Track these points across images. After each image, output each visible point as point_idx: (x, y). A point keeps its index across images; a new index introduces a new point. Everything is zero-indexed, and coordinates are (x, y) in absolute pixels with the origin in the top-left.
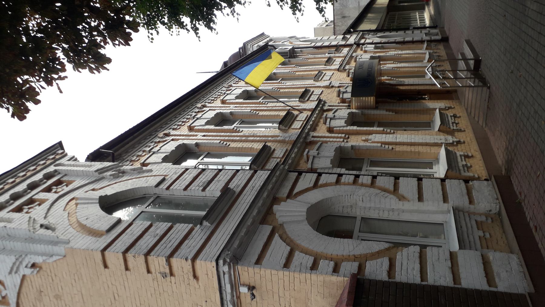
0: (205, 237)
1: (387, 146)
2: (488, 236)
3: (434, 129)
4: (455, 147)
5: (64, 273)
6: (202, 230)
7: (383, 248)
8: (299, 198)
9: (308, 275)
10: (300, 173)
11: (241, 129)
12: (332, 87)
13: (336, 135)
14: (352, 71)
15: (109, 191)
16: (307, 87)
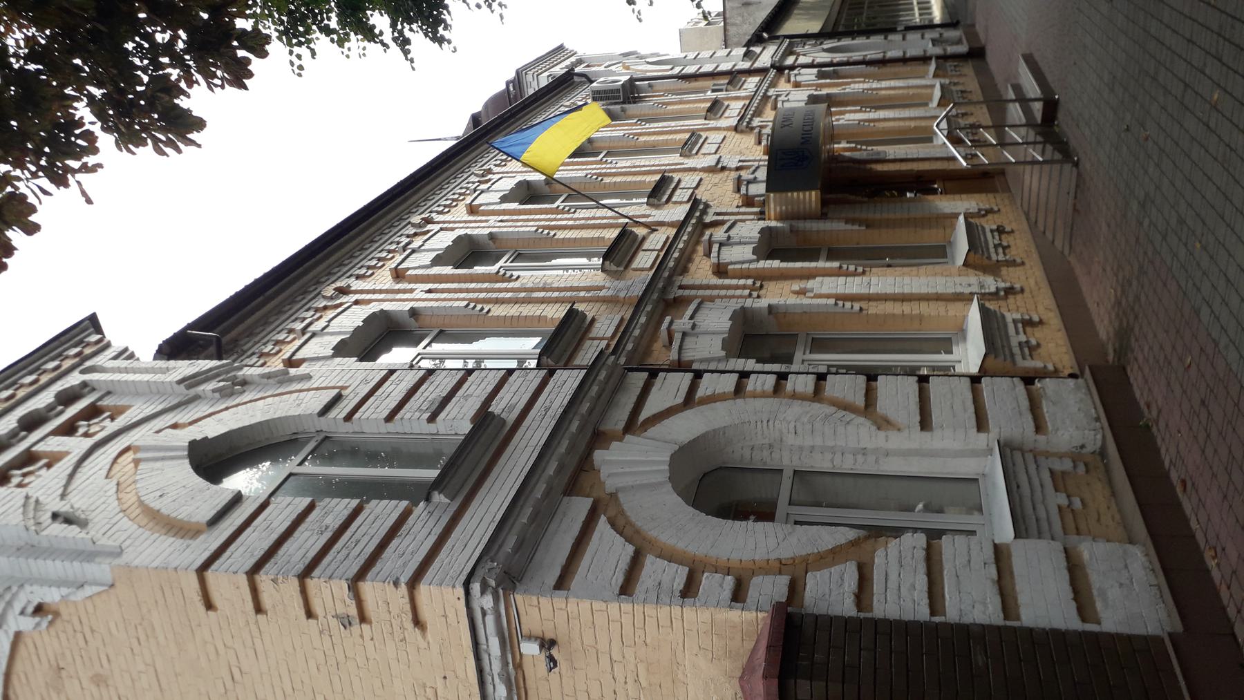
0: (438, 530)
1: (848, 305)
2: (1077, 503)
3: (954, 263)
4: (1002, 303)
5: (112, 625)
6: (431, 513)
7: (843, 541)
8: (653, 431)
9: (676, 610)
10: (653, 374)
11: (516, 274)
12: (723, 169)
13: (734, 282)
14: (768, 131)
15: (212, 428)
16: (665, 171)
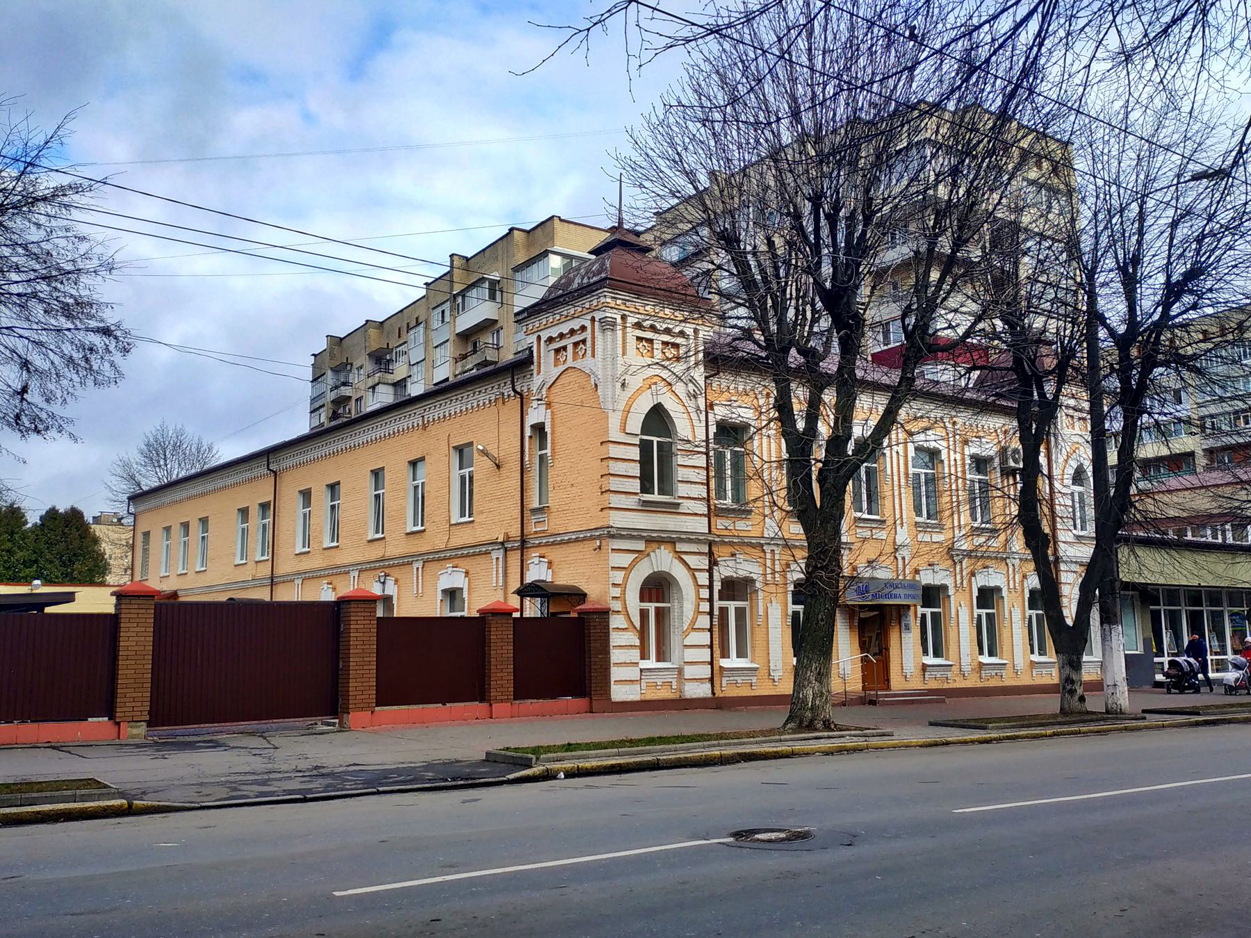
8: (676, 562)
